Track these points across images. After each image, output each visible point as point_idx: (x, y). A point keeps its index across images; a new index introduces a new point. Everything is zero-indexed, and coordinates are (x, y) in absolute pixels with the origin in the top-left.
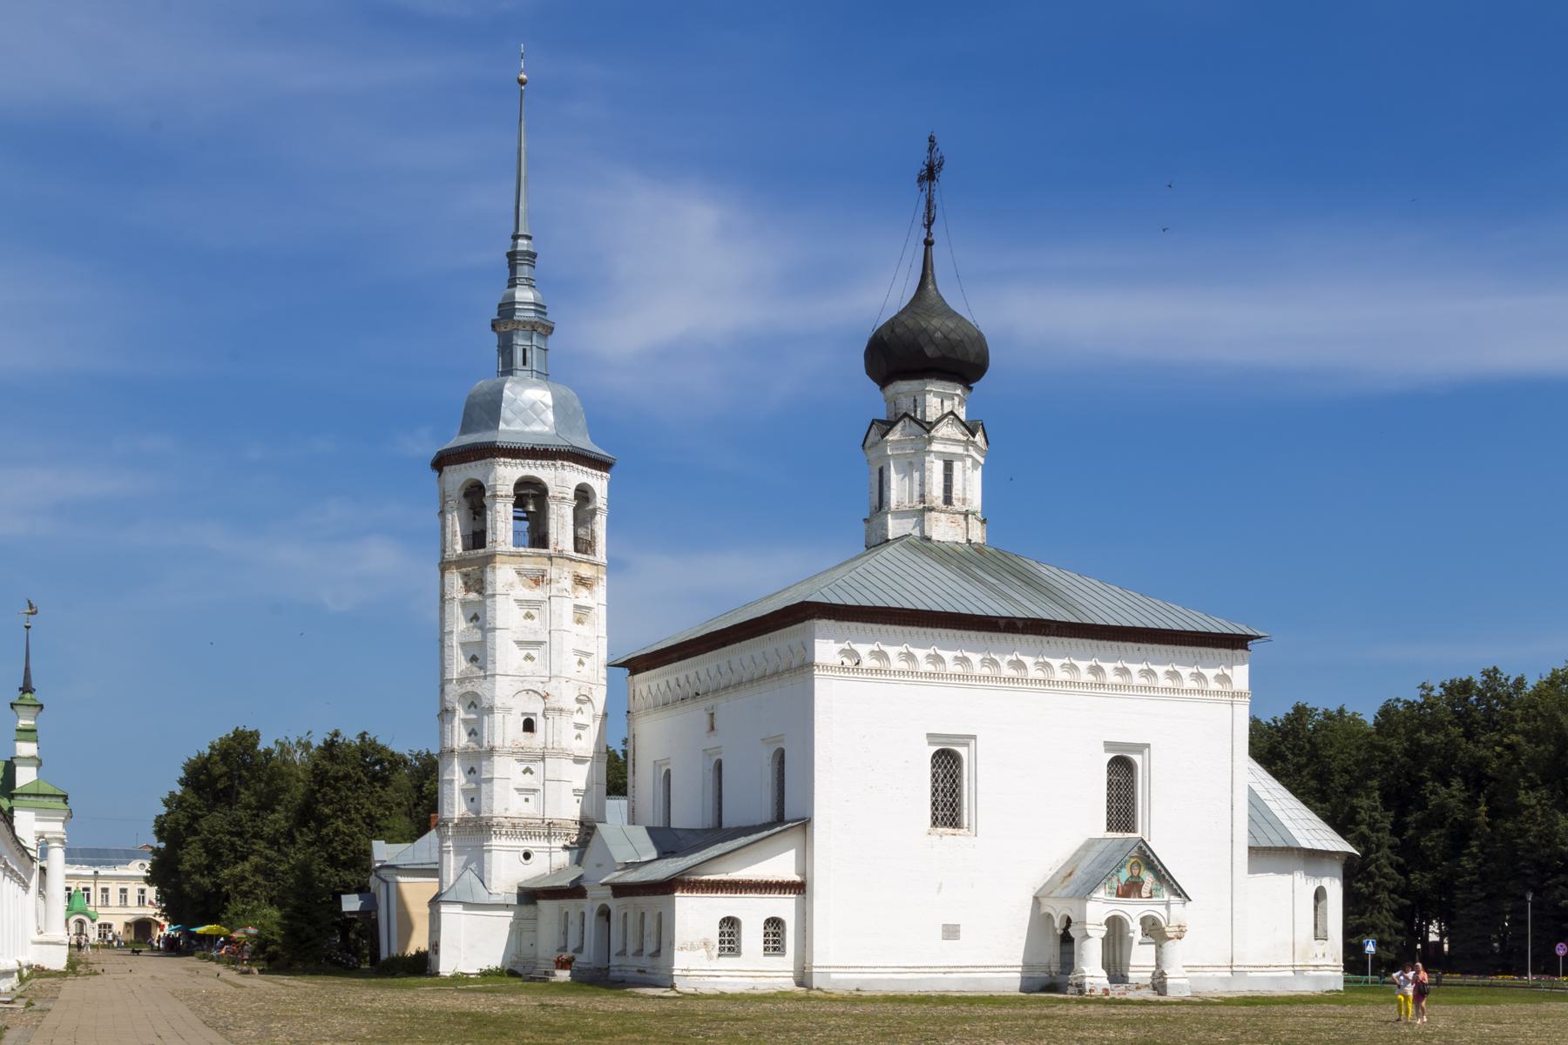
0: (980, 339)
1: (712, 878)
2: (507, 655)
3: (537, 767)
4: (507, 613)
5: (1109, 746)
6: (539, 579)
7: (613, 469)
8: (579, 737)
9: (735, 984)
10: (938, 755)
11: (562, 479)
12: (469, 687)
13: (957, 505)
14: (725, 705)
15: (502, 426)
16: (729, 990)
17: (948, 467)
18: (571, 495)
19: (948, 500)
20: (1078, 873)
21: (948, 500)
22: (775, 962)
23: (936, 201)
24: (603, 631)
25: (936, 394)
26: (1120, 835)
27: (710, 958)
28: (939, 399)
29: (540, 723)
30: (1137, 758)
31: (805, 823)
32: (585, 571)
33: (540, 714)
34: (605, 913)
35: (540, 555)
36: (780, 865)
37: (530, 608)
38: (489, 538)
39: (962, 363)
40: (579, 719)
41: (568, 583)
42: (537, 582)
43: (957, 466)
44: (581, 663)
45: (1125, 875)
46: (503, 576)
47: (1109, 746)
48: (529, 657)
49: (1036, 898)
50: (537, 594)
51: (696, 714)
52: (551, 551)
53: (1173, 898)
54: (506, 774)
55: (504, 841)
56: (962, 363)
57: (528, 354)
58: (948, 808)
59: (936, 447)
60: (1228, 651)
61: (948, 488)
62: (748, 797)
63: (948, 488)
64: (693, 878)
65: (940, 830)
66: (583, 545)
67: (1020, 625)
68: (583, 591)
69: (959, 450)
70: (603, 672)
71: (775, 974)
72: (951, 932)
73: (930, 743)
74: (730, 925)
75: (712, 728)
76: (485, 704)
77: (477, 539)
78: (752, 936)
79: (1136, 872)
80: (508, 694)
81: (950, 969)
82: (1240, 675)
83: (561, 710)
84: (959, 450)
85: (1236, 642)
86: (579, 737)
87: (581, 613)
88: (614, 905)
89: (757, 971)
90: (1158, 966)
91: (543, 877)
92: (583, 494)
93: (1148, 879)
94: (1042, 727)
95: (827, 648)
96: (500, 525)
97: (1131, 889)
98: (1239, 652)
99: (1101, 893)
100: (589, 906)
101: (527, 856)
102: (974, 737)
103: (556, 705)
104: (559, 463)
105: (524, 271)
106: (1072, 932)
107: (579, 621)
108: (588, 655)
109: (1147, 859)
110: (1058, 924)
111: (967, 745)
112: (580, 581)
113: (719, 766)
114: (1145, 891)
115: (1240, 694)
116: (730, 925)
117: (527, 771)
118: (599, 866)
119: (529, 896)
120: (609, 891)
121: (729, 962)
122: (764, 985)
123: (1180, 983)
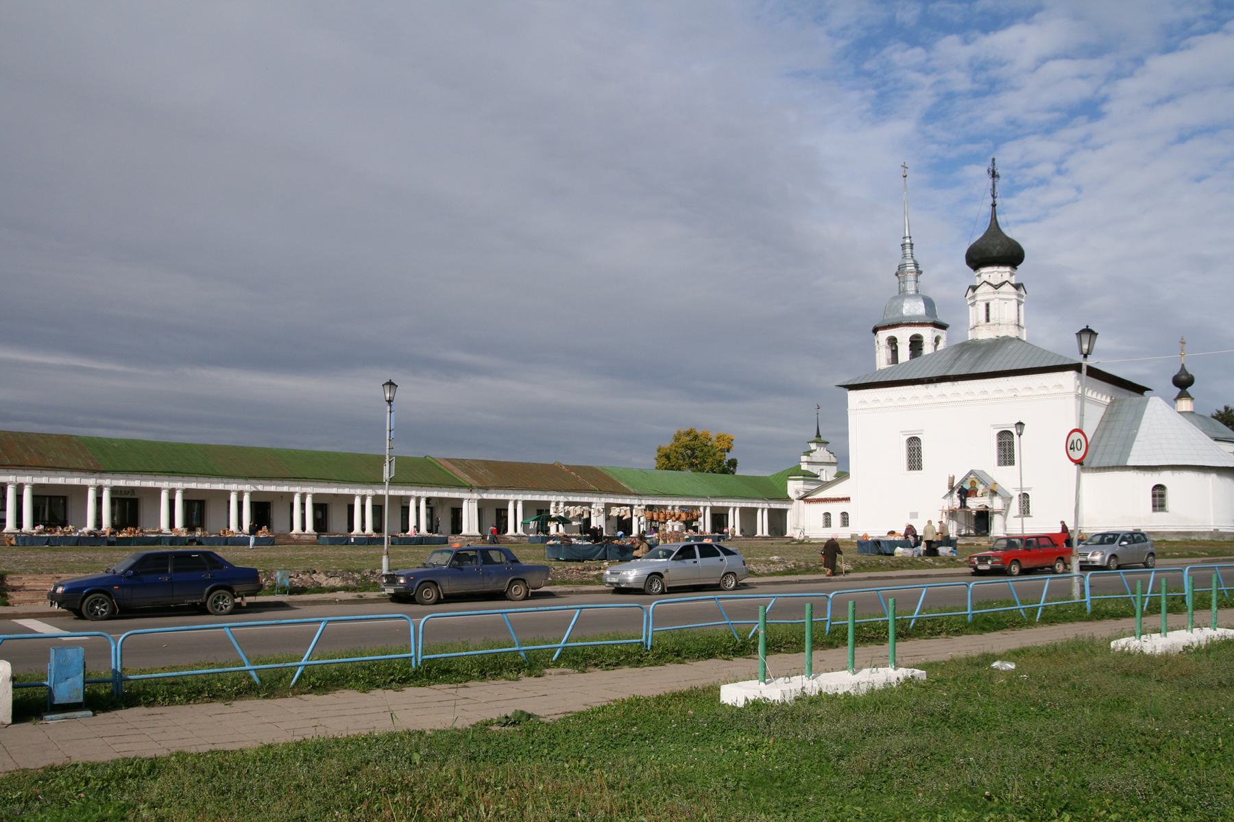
5: (994, 426)
11: (904, 336)
13: (992, 321)
17: (987, 305)
19: (988, 320)
21: (988, 320)
47: (994, 426)
59: (978, 298)
61: (988, 315)
63: (988, 315)
74: (827, 516)
78: (836, 520)
94: (959, 423)
105: (908, 251)
114: (979, 493)
116: (827, 515)
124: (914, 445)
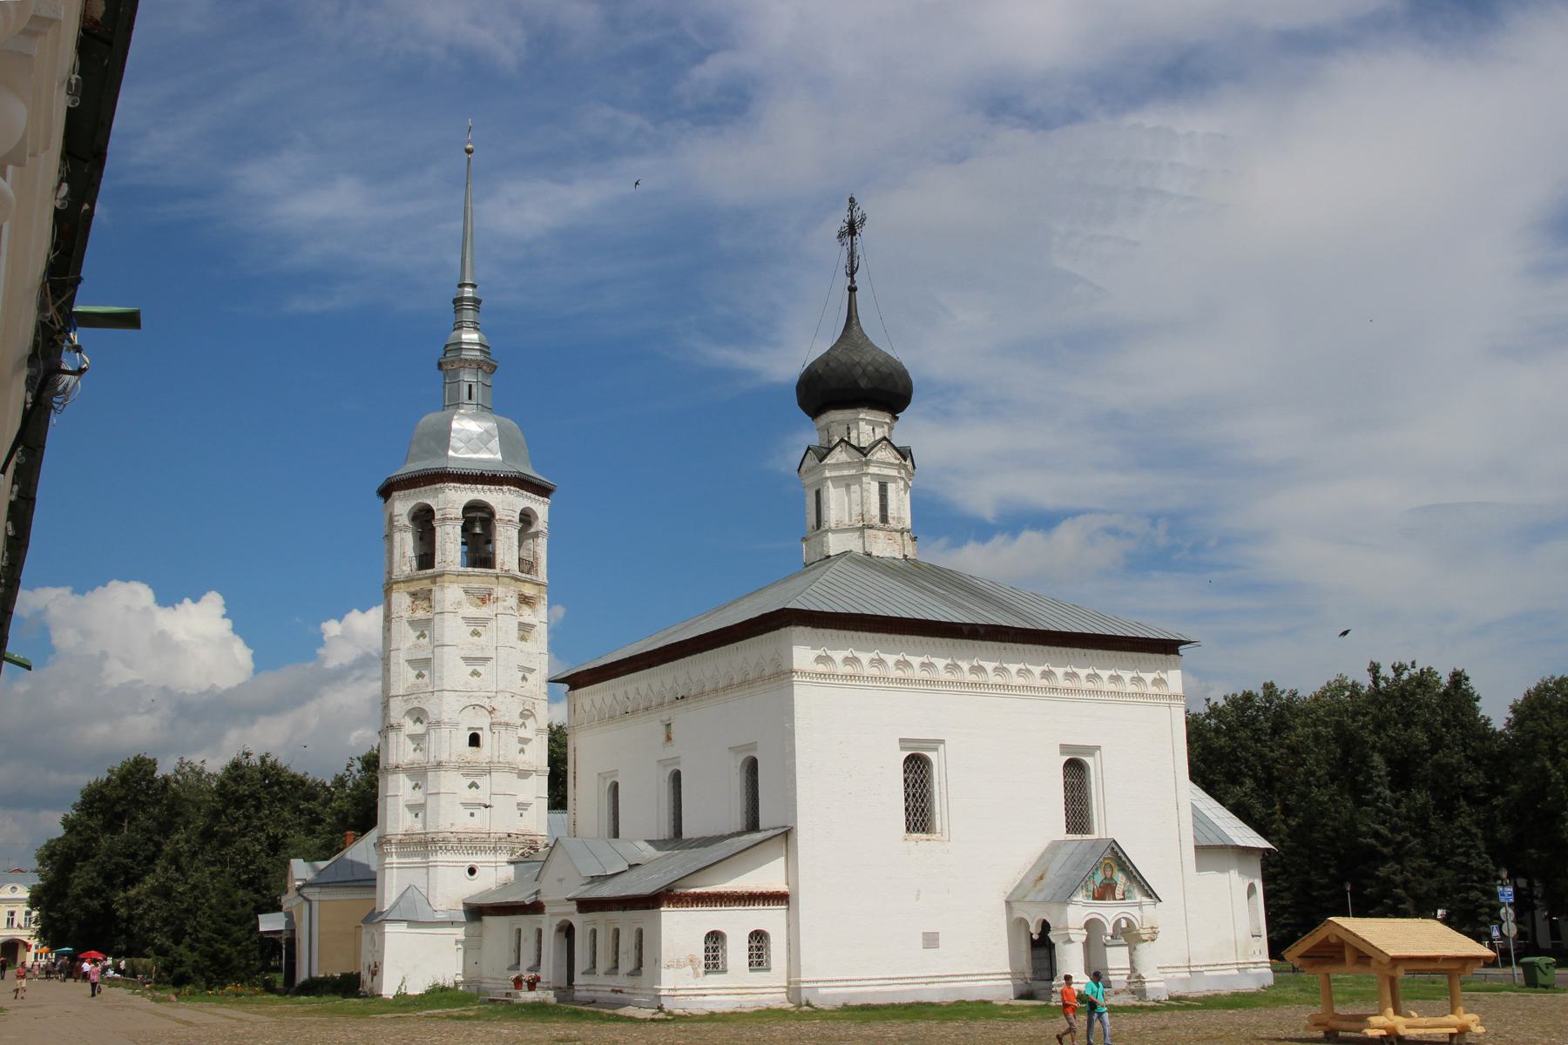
0: (904, 375)
1: (698, 890)
2: (453, 671)
3: (483, 781)
4: (453, 629)
5: (1064, 748)
6: (485, 598)
7: (553, 495)
8: (522, 751)
9: (722, 1003)
10: (909, 760)
11: (506, 503)
12: (416, 704)
13: (892, 523)
14: (683, 718)
15: (451, 453)
16: (718, 1009)
18: (517, 519)
19: (884, 518)
20: (1049, 877)
21: (884, 518)
22: (759, 978)
23: (859, 252)
24: (544, 647)
25: (868, 422)
26: (1079, 837)
27: (697, 976)
28: (867, 426)
29: (485, 738)
30: (1089, 760)
31: (786, 835)
32: (529, 590)
33: (486, 727)
34: (567, 931)
35: (487, 575)
36: (767, 876)
37: (477, 626)
38: (438, 558)
39: (888, 393)
40: (522, 733)
41: (513, 601)
42: (483, 601)
43: (891, 487)
44: (524, 678)
45: (1099, 878)
46: (451, 595)
47: (1064, 748)
48: (475, 673)
49: (1007, 903)
50: (484, 611)
51: (651, 727)
52: (497, 570)
53: (1145, 899)
54: (452, 784)
55: (450, 857)
56: (888, 393)
57: (474, 390)
58: (919, 816)
59: (873, 470)
60: (1163, 656)
62: (713, 806)
64: (678, 891)
65: (915, 835)
66: (527, 565)
67: (982, 631)
68: (526, 610)
69: (894, 473)
70: (545, 687)
71: (768, 989)
72: (931, 940)
73: (902, 749)
75: (669, 738)
76: (432, 718)
77: (426, 559)
78: (737, 951)
79: (1109, 874)
80: (454, 712)
81: (931, 979)
82: (1175, 679)
83: (507, 724)
84: (894, 473)
85: (1168, 647)
86: (522, 751)
87: (525, 629)
88: (580, 922)
89: (739, 988)
90: (1133, 969)
91: (489, 892)
92: (527, 518)
93: (1120, 878)
94: (1003, 728)
95: (803, 652)
96: (449, 546)
97: (1105, 892)
98: (1172, 657)
99: (1080, 897)
100: (548, 923)
101: (472, 871)
102: (942, 742)
103: (502, 720)
104: (505, 488)
105: (469, 315)
106: (1052, 936)
107: (523, 639)
108: (532, 670)
109: (1117, 859)
110: (1035, 929)
111: (936, 749)
112: (525, 600)
113: (676, 778)
115: (1176, 697)
117: (473, 785)
118: (560, 880)
119: (476, 912)
120: (574, 907)
121: (714, 980)
122: (749, 1003)
123: (1158, 985)
124: (917, 767)
